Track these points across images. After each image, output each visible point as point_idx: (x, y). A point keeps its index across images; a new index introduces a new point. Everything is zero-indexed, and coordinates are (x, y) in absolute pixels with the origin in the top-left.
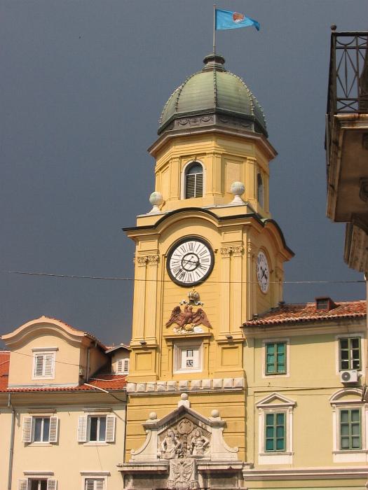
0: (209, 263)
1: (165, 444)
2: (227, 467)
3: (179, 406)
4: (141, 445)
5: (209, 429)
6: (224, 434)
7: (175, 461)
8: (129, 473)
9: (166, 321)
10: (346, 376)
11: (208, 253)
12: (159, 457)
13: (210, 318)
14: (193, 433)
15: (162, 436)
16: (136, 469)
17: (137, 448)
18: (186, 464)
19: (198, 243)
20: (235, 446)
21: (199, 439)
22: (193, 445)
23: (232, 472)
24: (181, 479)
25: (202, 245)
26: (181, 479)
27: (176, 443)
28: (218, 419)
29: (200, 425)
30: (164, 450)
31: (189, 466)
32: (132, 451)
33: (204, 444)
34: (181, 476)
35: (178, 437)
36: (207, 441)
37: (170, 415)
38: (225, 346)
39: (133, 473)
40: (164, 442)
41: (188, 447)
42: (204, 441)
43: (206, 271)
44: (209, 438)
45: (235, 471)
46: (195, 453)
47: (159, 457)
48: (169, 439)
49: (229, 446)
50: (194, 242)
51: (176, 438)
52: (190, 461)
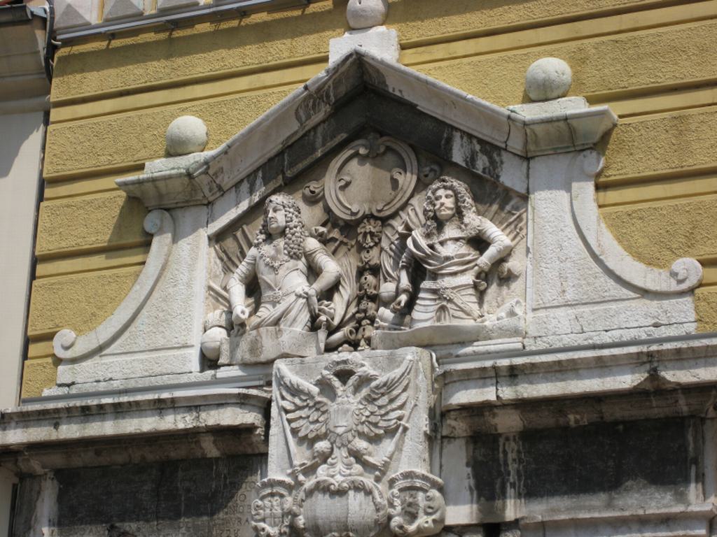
1: (253, 288)
2: (626, 381)
3: (335, 57)
4: (115, 301)
5: (510, 176)
6: (612, 196)
7: (304, 370)
8: (36, 465)
14: (418, 203)
15: (230, 243)
16: (70, 431)
17: (87, 322)
18: (366, 380)
20: (688, 246)
21: (451, 231)
22: (418, 270)
23: (658, 409)
24: (337, 472)
26: (337, 472)
27: (313, 272)
28: (574, 106)
29: (458, 156)
30: (241, 304)
31: (389, 386)
32: (66, 335)
33: (485, 259)
34: (339, 454)
35: (324, 240)
36: (499, 237)
37: (278, 119)
39: (58, 460)
40: (243, 268)
42: (479, 242)
44: (515, 226)
45: (683, 406)
46: (424, 314)
47: (209, 361)
48: (267, 249)
49: (639, 257)
51: (312, 244)
52: (392, 362)
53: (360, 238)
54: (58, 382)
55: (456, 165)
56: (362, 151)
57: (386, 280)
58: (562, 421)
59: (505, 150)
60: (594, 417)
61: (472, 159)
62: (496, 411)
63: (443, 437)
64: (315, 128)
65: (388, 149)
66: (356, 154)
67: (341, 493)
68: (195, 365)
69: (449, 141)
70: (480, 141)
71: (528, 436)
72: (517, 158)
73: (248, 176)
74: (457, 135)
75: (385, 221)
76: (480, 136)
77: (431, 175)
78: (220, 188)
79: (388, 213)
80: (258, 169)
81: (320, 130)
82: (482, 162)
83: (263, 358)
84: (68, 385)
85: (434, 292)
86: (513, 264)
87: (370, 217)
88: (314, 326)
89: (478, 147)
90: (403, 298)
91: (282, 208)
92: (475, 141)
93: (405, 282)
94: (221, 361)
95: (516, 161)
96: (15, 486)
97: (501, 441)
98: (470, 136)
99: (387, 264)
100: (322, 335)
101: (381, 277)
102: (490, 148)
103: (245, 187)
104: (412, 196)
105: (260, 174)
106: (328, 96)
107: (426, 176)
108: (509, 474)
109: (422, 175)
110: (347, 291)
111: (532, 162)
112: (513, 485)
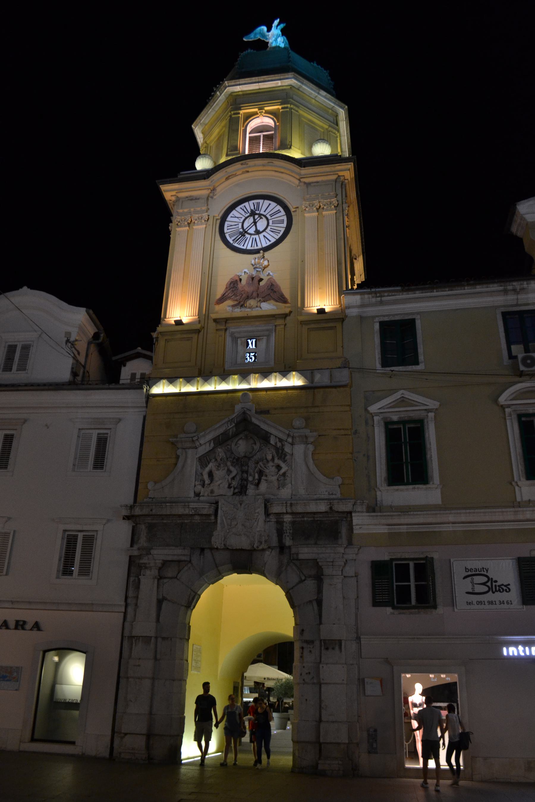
0: (285, 225)
1: (211, 474)
5: (287, 449)
9: (218, 296)
10: (529, 361)
11: (283, 212)
12: (197, 495)
13: (287, 293)
19: (267, 202)
21: (271, 464)
25: (273, 204)
29: (272, 442)
38: (313, 326)
40: (207, 469)
41: (250, 479)
42: (279, 467)
43: (280, 235)
47: (197, 495)
50: (261, 201)
53: (242, 462)
54: (149, 496)
55: (271, 444)
56: (243, 437)
57: (250, 476)
58: (303, 519)
59: (286, 441)
60: (312, 519)
61: (276, 443)
62: (284, 515)
63: (268, 521)
64: (229, 429)
65: (251, 438)
66: (241, 438)
67: (240, 535)
68: (192, 495)
69: (270, 437)
70: (279, 438)
71: (293, 523)
72: (289, 444)
73: (208, 441)
74: (272, 436)
75: (249, 458)
76: (279, 437)
77: (264, 447)
78: (200, 444)
79: (251, 456)
80: (212, 439)
81: (231, 430)
82: (279, 445)
83: (214, 495)
84: (152, 498)
85: (266, 480)
86: (288, 474)
87: (245, 457)
88: (229, 487)
89: (278, 440)
90: (257, 481)
91: (221, 452)
92: (277, 438)
93: (257, 476)
94: (201, 495)
95: (289, 445)
96: (133, 527)
97: (285, 524)
98: (276, 437)
99: (251, 471)
100: (232, 489)
101: (249, 474)
102: (281, 440)
103: (208, 444)
104: (258, 452)
105: (212, 441)
106: (234, 421)
107: (262, 446)
108: (287, 533)
109: (261, 446)
110: (238, 478)
111: (294, 445)
112: (288, 536)
